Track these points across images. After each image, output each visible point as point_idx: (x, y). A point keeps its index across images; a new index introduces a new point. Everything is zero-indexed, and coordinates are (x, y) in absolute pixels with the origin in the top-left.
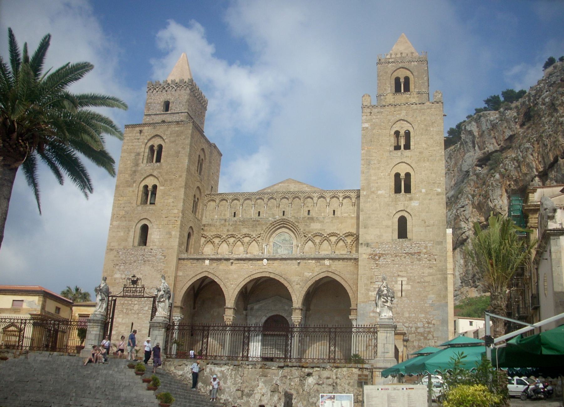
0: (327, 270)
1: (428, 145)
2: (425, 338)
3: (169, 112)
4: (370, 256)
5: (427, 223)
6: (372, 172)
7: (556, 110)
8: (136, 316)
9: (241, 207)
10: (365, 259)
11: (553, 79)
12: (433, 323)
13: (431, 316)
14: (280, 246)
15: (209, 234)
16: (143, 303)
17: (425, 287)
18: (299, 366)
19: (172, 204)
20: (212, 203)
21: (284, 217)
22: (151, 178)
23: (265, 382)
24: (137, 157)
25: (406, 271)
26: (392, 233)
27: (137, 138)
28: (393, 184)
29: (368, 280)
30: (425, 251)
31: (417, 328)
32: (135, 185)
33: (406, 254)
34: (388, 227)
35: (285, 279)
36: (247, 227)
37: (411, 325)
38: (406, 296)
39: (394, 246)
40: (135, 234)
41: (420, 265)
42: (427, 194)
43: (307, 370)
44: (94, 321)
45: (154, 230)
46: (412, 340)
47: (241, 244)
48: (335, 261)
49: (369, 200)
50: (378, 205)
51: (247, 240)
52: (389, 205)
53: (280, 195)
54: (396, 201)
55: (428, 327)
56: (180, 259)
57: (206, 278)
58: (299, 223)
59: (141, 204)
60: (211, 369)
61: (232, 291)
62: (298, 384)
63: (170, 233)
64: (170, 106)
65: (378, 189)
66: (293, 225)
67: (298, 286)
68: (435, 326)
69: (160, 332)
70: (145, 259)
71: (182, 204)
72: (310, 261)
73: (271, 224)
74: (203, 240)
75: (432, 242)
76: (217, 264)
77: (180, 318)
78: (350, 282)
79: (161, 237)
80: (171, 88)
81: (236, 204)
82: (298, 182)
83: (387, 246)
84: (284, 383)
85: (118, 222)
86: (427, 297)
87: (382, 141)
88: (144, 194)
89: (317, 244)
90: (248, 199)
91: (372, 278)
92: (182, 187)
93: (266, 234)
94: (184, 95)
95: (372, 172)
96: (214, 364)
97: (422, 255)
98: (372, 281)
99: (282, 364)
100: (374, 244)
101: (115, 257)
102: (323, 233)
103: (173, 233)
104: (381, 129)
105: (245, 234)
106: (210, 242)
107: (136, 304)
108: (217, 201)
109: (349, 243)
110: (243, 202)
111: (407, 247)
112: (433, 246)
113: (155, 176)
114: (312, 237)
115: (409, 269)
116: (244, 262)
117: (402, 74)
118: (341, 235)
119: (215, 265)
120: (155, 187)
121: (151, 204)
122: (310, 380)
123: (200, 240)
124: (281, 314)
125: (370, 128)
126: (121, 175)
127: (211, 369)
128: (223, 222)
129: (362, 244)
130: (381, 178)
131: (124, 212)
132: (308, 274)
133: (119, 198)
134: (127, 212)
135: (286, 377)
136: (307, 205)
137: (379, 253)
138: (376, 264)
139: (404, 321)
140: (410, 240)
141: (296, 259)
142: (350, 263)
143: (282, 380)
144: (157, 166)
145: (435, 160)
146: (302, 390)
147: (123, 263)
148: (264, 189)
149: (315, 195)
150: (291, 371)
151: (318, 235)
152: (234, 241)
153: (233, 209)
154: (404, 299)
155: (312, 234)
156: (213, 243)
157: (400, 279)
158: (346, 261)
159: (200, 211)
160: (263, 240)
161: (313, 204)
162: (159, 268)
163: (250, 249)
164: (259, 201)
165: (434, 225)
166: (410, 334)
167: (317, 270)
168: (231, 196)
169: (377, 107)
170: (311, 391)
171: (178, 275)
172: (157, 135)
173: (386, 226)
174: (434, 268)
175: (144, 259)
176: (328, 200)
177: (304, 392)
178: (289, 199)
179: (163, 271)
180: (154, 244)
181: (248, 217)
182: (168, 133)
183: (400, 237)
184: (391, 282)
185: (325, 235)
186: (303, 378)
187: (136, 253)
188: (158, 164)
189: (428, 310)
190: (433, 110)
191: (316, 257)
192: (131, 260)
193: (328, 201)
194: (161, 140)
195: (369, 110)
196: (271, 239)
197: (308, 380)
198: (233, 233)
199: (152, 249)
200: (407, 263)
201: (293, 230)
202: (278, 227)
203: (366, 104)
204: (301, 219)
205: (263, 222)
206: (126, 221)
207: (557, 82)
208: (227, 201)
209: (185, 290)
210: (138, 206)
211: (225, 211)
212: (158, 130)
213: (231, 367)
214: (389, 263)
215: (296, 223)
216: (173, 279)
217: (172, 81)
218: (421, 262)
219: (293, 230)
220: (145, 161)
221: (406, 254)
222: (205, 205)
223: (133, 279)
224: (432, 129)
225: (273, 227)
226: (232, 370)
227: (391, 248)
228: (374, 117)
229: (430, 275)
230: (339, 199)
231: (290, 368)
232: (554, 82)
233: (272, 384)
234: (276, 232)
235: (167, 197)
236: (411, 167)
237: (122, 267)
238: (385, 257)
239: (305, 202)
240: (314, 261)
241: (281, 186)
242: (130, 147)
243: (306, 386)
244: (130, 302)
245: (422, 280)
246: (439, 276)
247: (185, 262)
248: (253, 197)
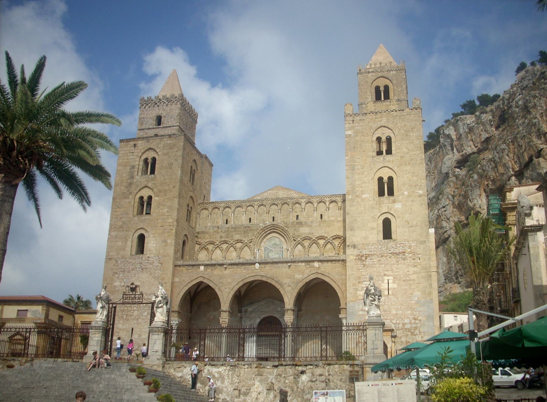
0: (316, 272)
1: (409, 150)
2: (412, 334)
3: (161, 126)
4: (357, 257)
5: (410, 224)
6: (356, 177)
7: (529, 112)
9: (233, 215)
10: (353, 260)
11: (525, 83)
12: (419, 318)
13: (418, 312)
14: (271, 250)
15: (203, 241)
16: (142, 309)
17: (410, 285)
18: (293, 365)
19: (167, 214)
20: (205, 212)
21: (274, 223)
22: (146, 189)
23: (260, 381)
24: (132, 170)
25: (392, 270)
26: (378, 234)
27: (131, 151)
28: (376, 188)
29: (356, 280)
30: (409, 250)
31: (404, 325)
32: (131, 196)
33: (391, 254)
34: (373, 229)
36: (239, 233)
37: (398, 322)
38: (393, 294)
39: (380, 247)
40: (132, 243)
41: (405, 264)
42: (409, 196)
43: (300, 368)
44: (96, 328)
46: (400, 336)
47: (233, 249)
48: (324, 263)
49: (354, 204)
50: (363, 208)
51: (239, 245)
52: (373, 208)
53: (270, 202)
54: (380, 204)
55: (415, 323)
56: (176, 266)
57: (201, 283)
58: (288, 228)
59: (137, 214)
60: (209, 370)
61: (227, 294)
62: (292, 381)
63: (165, 242)
64: (162, 120)
65: (363, 193)
66: (283, 230)
67: (290, 288)
68: (422, 321)
69: (159, 336)
70: (143, 267)
71: (176, 213)
72: (300, 264)
73: (262, 229)
74: (197, 247)
75: (416, 242)
76: (212, 270)
77: (177, 322)
78: (339, 283)
79: (157, 245)
80: (162, 103)
81: (228, 212)
82: (287, 189)
83: (373, 247)
84: (279, 382)
85: (116, 233)
86: (412, 294)
87: (365, 147)
88: (139, 205)
89: (306, 247)
90: (239, 207)
91: (359, 278)
92: (176, 197)
93: (258, 240)
94: (175, 109)
95: (356, 177)
96: (212, 365)
97: (406, 255)
98: (359, 281)
99: (276, 363)
101: (114, 265)
102: (312, 237)
103: (169, 241)
104: (364, 136)
105: (237, 240)
106: (204, 249)
107: (136, 310)
108: (210, 210)
109: (336, 245)
110: (235, 210)
111: (392, 247)
112: (417, 246)
113: (150, 188)
114: (301, 241)
115: (394, 269)
116: (238, 267)
117: (381, 83)
118: (329, 238)
119: (209, 270)
120: (150, 198)
121: (146, 214)
122: (304, 378)
123: (194, 247)
124: (274, 315)
125: (353, 135)
126: (117, 187)
127: (209, 370)
128: (216, 229)
129: (349, 246)
130: (365, 183)
131: (121, 222)
132: (298, 276)
133: (117, 210)
134: (124, 223)
135: (280, 375)
136: (295, 211)
139: (392, 318)
140: (395, 240)
141: (287, 262)
143: (277, 378)
144: (152, 177)
145: (416, 164)
146: (296, 388)
147: (122, 272)
148: (254, 197)
149: (303, 200)
150: (285, 369)
151: (307, 239)
152: (227, 247)
153: (225, 217)
154: (391, 297)
155: (301, 237)
156: (207, 249)
157: (386, 278)
158: (334, 262)
159: (194, 219)
160: (254, 245)
161: (301, 209)
162: (156, 275)
163: (243, 254)
164: (249, 208)
165: (417, 226)
166: (397, 330)
167: (307, 272)
168: (223, 205)
169: (359, 115)
170: (305, 388)
171: (175, 281)
172: (151, 149)
173: (371, 228)
174: (419, 266)
175: (141, 267)
176: (315, 205)
177: (299, 390)
178: (279, 206)
179: (160, 278)
180: (151, 252)
181: (240, 223)
182: (161, 146)
183: (384, 239)
184: (378, 281)
185: (314, 239)
186: (297, 375)
188: (152, 175)
189: (414, 307)
190: (413, 116)
191: (306, 259)
192: (129, 268)
193: (315, 206)
194: (155, 153)
195: (351, 118)
196: (262, 244)
197: (302, 378)
198: (226, 239)
199: (149, 257)
200: (392, 262)
201: (283, 235)
202: (269, 232)
203: (349, 113)
204: (291, 224)
205: (254, 228)
206: (123, 231)
207: (529, 86)
208: (219, 209)
209: (182, 295)
210: (134, 216)
211: (218, 219)
212: (151, 143)
213: (228, 368)
214: (376, 263)
215: (285, 228)
217: (163, 96)
218: (406, 261)
219: (283, 235)
220: (140, 174)
221: (391, 254)
222: (199, 214)
223: (131, 287)
224: (412, 135)
225: (264, 232)
226: (229, 370)
228: (357, 124)
229: (415, 273)
230: (325, 203)
231: (284, 367)
232: (527, 86)
233: (268, 382)
234: (267, 237)
235: (161, 207)
236: (393, 170)
237: (121, 275)
238: (371, 258)
239: (294, 207)
240: (303, 264)
241: (270, 194)
242: (125, 161)
243: (300, 384)
244: (130, 309)
245: (408, 278)
246: (424, 274)
247: (181, 268)
248: (244, 204)
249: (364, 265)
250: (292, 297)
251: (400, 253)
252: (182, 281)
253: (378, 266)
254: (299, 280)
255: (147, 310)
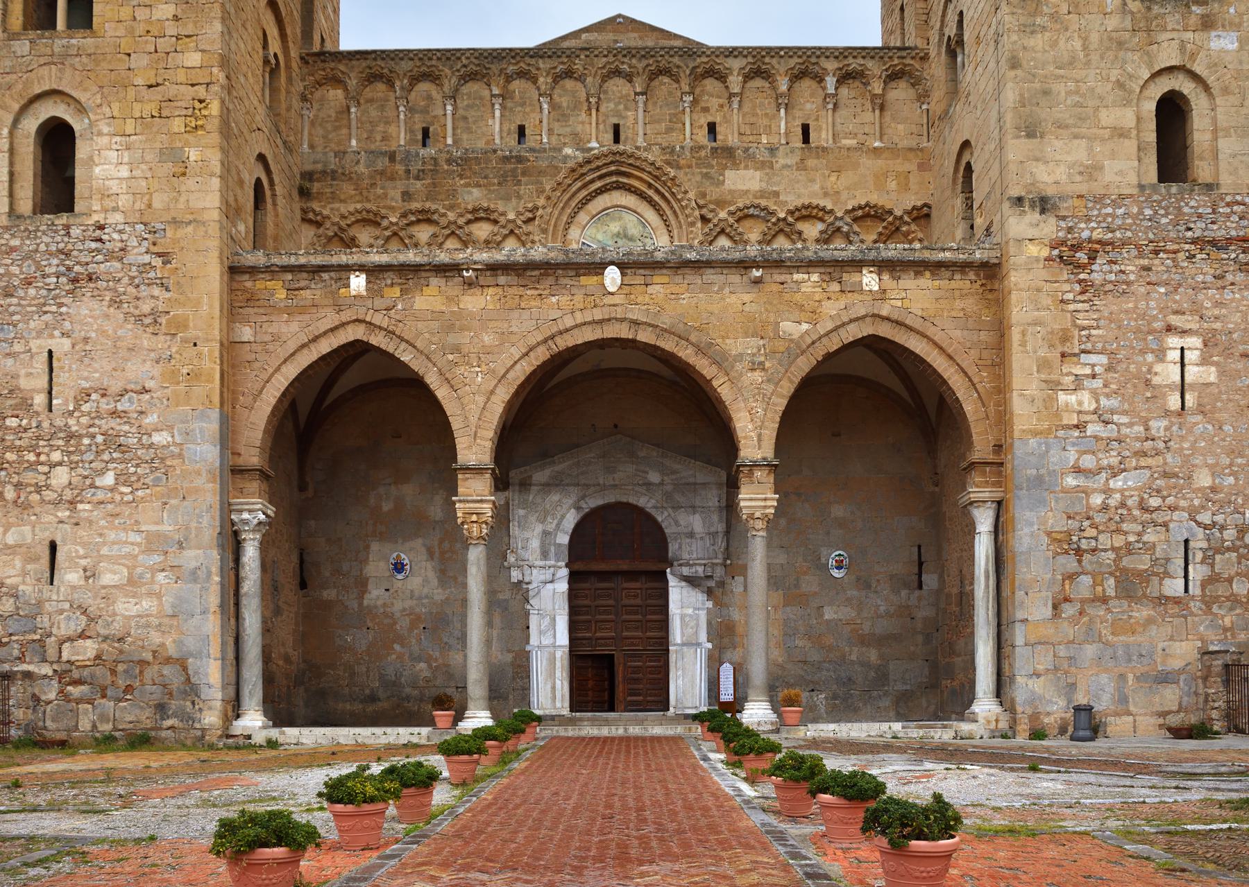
4: (1056, 252)
8: (64, 514)
10: (1037, 260)
16: (89, 456)
29: (1052, 346)
33: (1194, 241)
35: (700, 350)
39: (1148, 212)
45: (105, 140)
52: (1120, 44)
54: (1149, 30)
61: (480, 400)
67: (758, 376)
77: (262, 517)
100: (1070, 203)
107: (60, 464)
111: (1200, 216)
115: (1208, 304)
129: (1019, 200)
132: (793, 328)
136: (703, 104)
137: (1090, 240)
138: (1080, 282)
142: (961, 283)
162: (146, 308)
175: (69, 269)
179: (163, 320)
180: (109, 203)
187: (29, 245)
200: (1200, 278)
209: (273, 401)
214: (1132, 277)
216: (217, 354)
227: (1135, 217)
244: (32, 457)
249: (1085, 286)
250: (769, 415)
251: (1230, 240)
252: (268, 338)
253: (1142, 290)
254: (798, 345)
255: (113, 460)
